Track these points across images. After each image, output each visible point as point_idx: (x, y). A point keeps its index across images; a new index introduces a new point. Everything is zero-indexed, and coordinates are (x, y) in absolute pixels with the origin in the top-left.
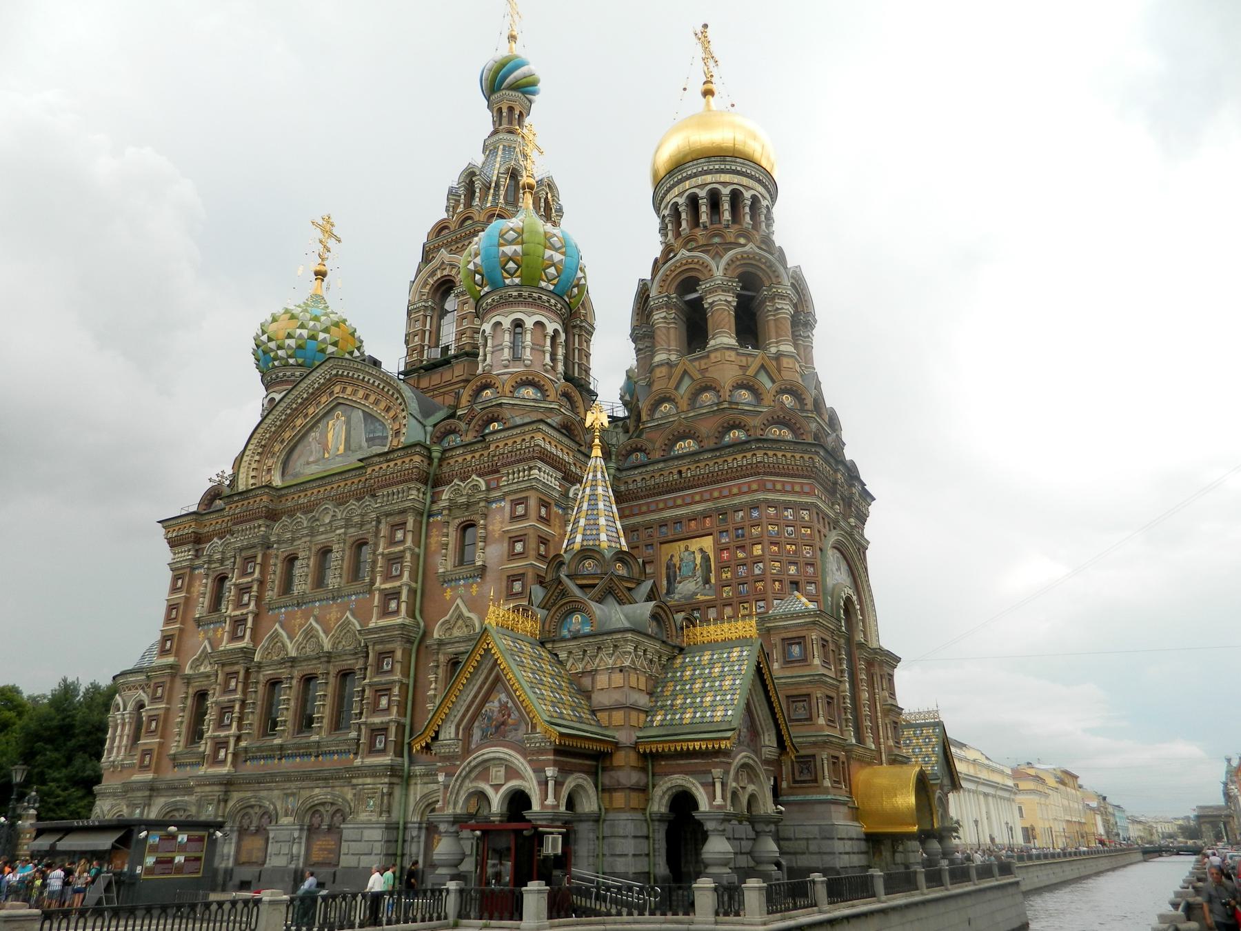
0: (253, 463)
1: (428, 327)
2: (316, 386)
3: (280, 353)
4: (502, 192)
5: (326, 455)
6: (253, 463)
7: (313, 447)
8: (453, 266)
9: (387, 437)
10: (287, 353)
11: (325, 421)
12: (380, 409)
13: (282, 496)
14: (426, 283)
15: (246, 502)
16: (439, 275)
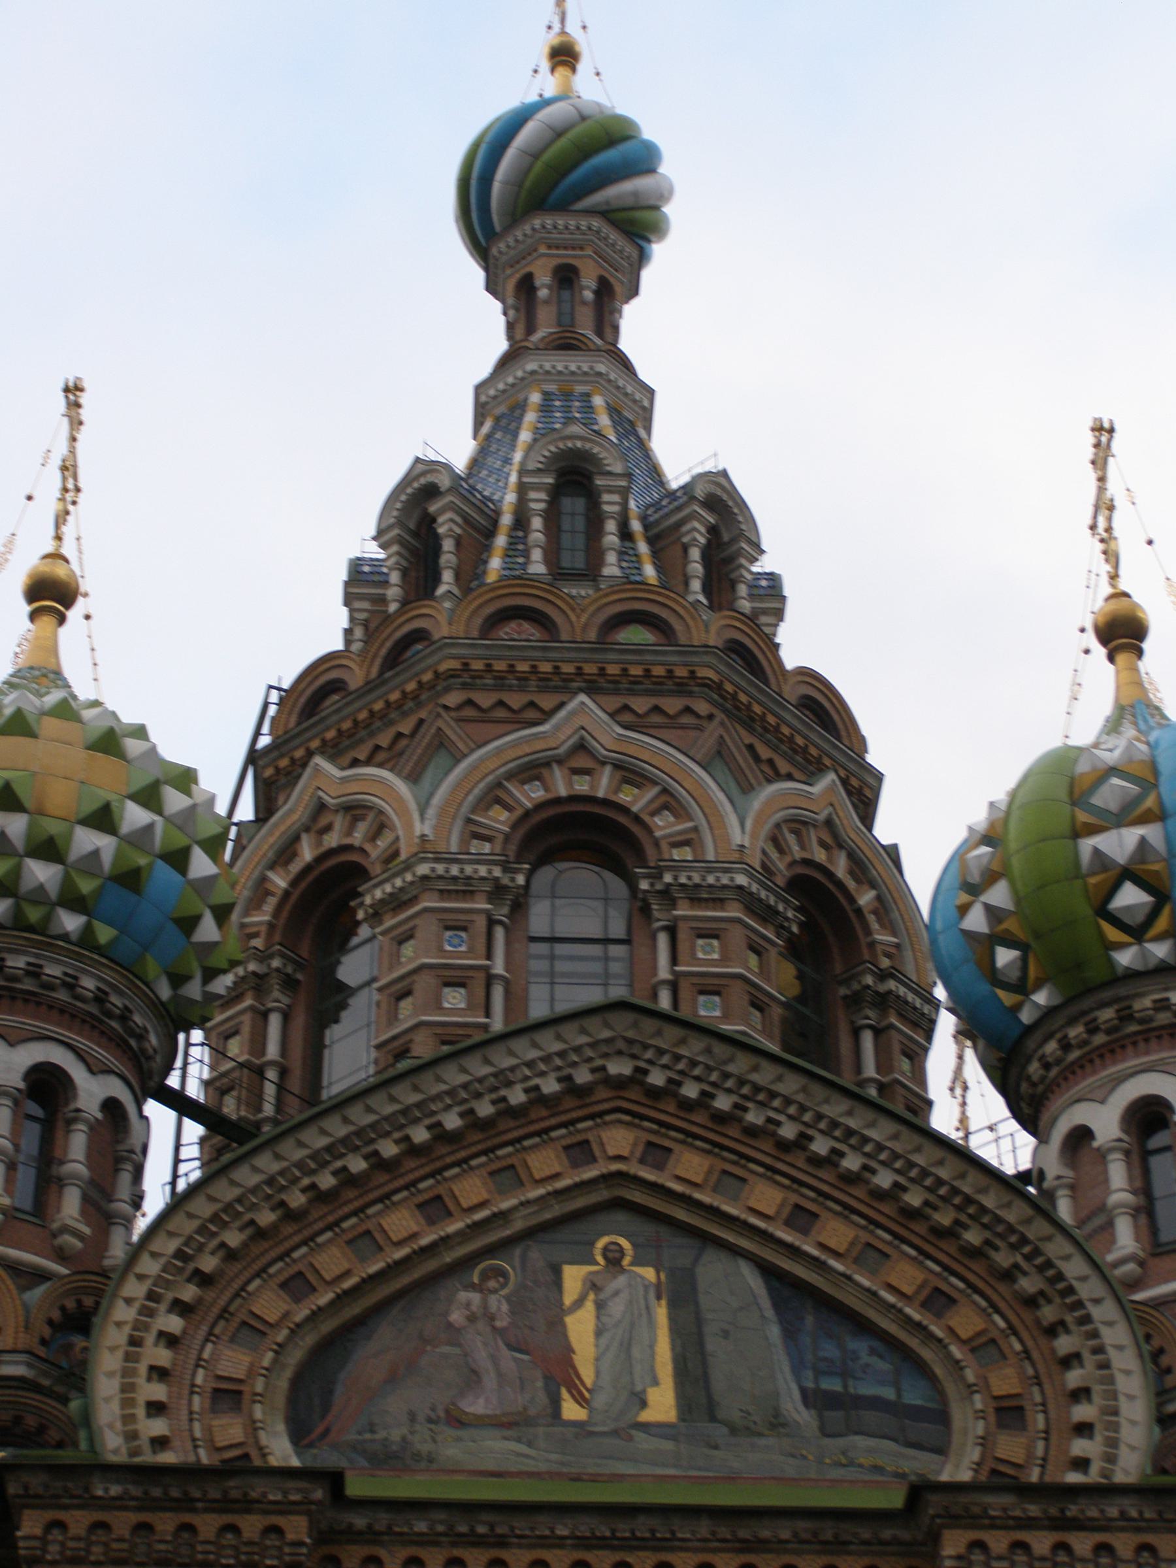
0: (150, 1339)
1: (499, 968)
2: (517, 1097)
3: (41, 873)
4: (696, 567)
5: (571, 1410)
6: (150, 1339)
7: (481, 1357)
8: (630, 774)
9: (943, 1418)
10: (67, 883)
11: (537, 1255)
12: (891, 1288)
13: (352, 1536)
14: (494, 797)
15: (165, 1523)
16: (561, 785)
